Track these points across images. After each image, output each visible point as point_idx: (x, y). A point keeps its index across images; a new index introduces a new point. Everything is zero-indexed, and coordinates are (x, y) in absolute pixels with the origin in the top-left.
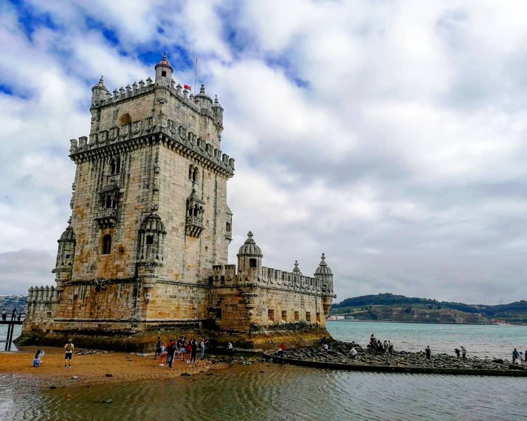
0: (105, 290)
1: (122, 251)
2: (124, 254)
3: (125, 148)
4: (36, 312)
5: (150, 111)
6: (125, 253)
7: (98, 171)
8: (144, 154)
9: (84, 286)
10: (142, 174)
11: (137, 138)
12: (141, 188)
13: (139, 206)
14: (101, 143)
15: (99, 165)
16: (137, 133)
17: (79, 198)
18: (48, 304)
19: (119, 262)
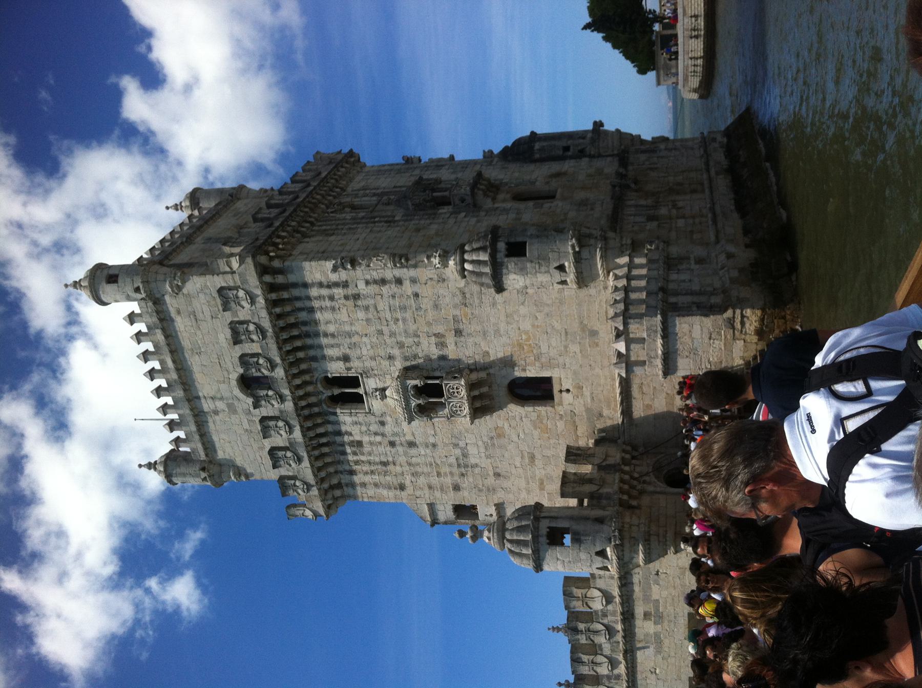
1: (558, 175)
4: (696, 287)
6: (563, 170)
11: (332, 170)
16: (320, 173)
18: (670, 263)
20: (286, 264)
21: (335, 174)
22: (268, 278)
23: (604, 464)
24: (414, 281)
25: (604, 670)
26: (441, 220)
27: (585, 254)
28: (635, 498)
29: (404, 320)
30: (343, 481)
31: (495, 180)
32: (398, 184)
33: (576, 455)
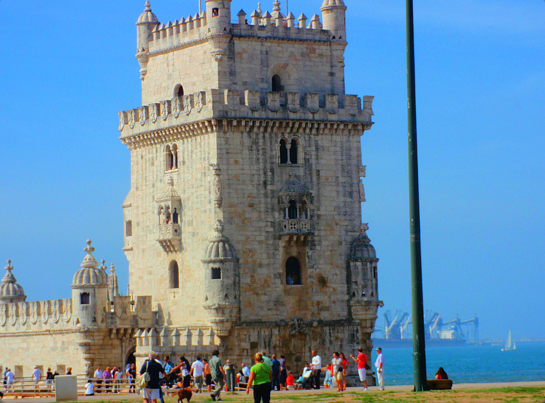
0: (305, 335)
1: (323, 281)
2: (327, 287)
3: (311, 129)
5: (327, 74)
6: (328, 285)
7: (261, 152)
8: (339, 145)
9: (266, 330)
10: (339, 174)
12: (341, 195)
13: (340, 220)
14: (272, 111)
15: (260, 144)
17: (231, 191)
19: (319, 297)
20: (216, 133)
21: (332, 125)
22: (207, 124)
23: (138, 318)
24: (210, 211)
25: (43, 319)
26: (263, 216)
27: (213, 311)
28: (118, 337)
29: (197, 202)
30: (138, 149)
31: (320, 241)
32: (322, 173)
33: (144, 302)
